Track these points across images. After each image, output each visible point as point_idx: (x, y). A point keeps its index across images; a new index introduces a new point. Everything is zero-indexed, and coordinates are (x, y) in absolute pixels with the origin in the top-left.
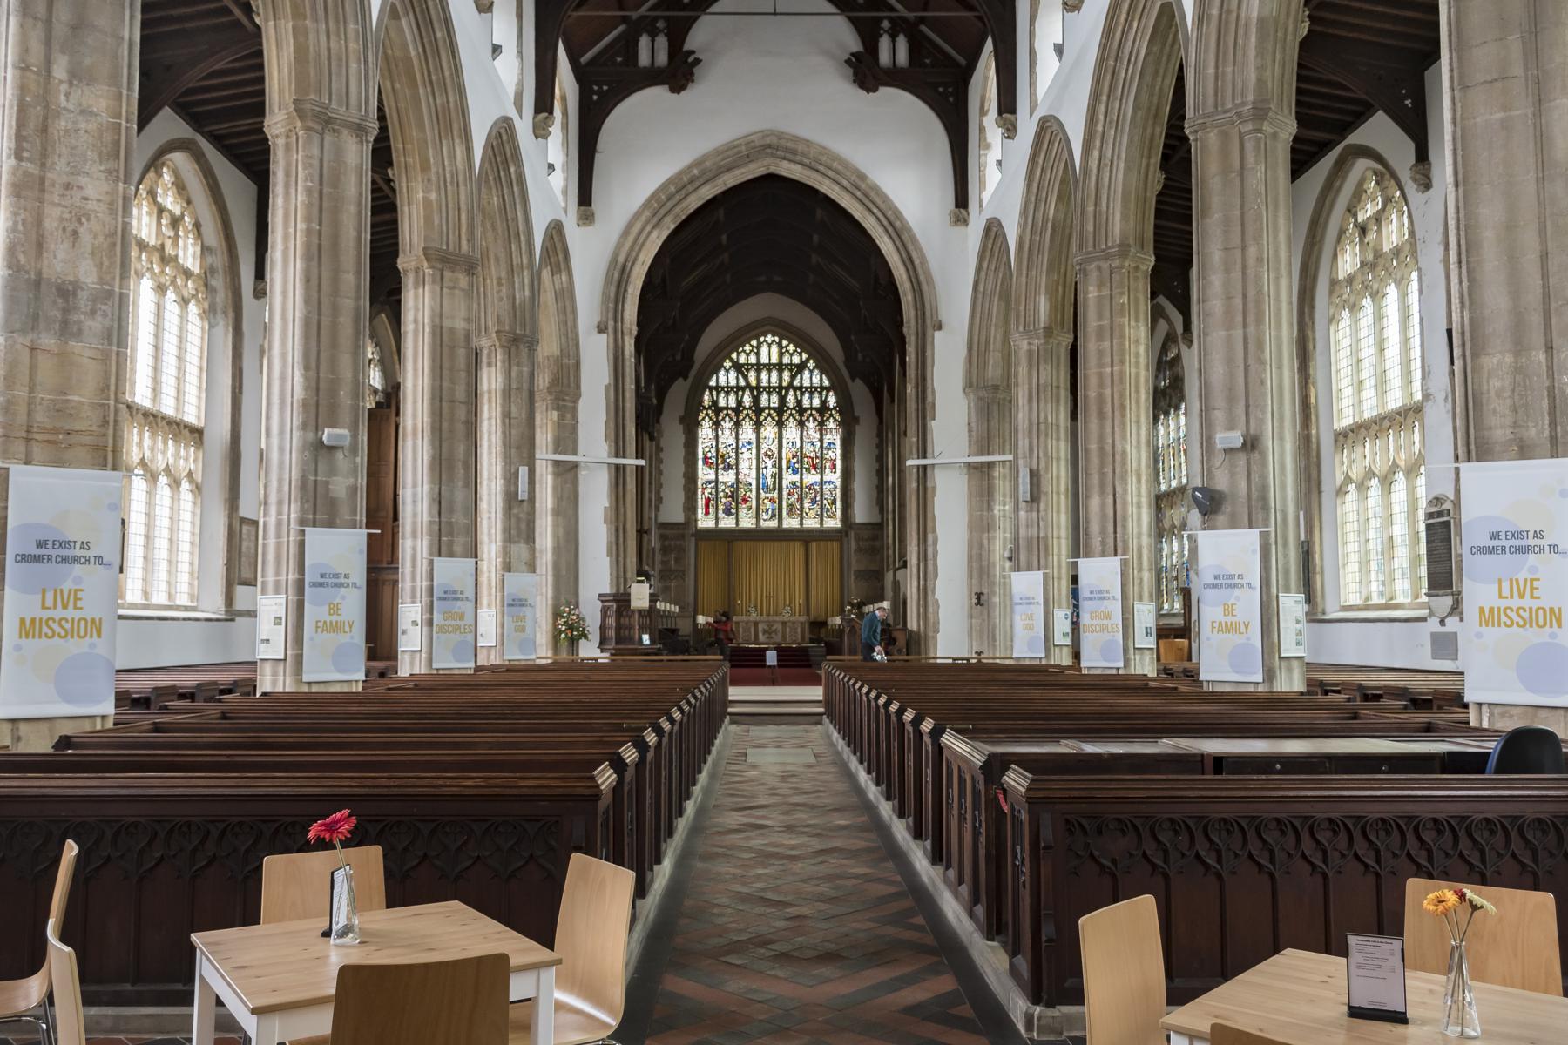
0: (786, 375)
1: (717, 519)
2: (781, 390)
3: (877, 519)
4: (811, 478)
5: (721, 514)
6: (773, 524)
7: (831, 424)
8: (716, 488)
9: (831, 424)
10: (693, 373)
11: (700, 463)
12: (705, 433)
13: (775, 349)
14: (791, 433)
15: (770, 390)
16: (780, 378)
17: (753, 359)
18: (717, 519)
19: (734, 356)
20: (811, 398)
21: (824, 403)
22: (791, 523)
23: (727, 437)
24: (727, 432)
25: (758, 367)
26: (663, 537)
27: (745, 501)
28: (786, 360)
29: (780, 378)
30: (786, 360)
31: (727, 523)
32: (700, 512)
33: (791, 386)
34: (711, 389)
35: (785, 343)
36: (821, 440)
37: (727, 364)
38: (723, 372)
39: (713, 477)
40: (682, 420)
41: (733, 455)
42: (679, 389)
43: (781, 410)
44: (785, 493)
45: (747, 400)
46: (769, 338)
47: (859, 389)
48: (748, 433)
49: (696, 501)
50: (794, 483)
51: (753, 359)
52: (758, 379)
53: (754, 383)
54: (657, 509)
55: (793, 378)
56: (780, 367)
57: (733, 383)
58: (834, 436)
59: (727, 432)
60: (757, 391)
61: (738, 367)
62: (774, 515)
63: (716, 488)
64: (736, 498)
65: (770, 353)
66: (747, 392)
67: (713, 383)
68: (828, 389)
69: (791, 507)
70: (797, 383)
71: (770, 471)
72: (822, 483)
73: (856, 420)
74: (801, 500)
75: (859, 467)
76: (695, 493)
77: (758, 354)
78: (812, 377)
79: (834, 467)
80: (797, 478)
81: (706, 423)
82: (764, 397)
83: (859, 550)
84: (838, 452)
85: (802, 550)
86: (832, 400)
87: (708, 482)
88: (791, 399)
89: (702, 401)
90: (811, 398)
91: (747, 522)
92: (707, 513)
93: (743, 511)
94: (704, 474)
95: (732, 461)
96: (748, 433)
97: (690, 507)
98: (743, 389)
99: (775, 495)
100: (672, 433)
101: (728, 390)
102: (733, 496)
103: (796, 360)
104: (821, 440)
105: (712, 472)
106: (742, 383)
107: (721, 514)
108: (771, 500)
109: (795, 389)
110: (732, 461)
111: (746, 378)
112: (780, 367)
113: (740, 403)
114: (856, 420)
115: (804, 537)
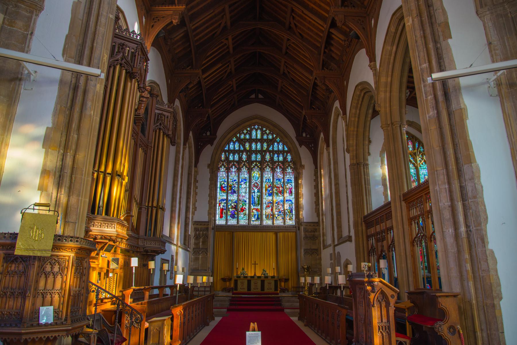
0: (265, 145)
1: (227, 220)
2: (262, 152)
3: (317, 221)
5: (229, 218)
6: (258, 223)
7: (289, 170)
8: (227, 203)
9: (289, 170)
10: (215, 142)
11: (218, 189)
12: (222, 174)
13: (259, 132)
14: (268, 175)
15: (256, 152)
16: (262, 146)
17: (248, 137)
18: (227, 220)
19: (238, 135)
20: (278, 157)
21: (285, 159)
22: (267, 222)
23: (233, 176)
24: (234, 174)
25: (251, 141)
26: (196, 230)
27: (242, 210)
28: (265, 137)
29: (262, 146)
30: (265, 137)
31: (232, 222)
32: (218, 217)
33: (268, 150)
34: (225, 151)
35: (264, 129)
37: (235, 139)
38: (232, 143)
39: (225, 197)
40: (209, 166)
41: (237, 186)
42: (208, 151)
43: (263, 162)
44: (265, 206)
45: (244, 157)
46: (256, 127)
47: (304, 153)
48: (245, 175)
49: (215, 210)
51: (248, 137)
52: (250, 147)
53: (248, 149)
54: (193, 213)
55: (268, 146)
56: (262, 141)
57: (237, 148)
58: (290, 176)
59: (234, 174)
60: (250, 152)
61: (240, 141)
62: (258, 218)
63: (227, 203)
64: (236, 210)
65: (257, 134)
66: (245, 154)
67: (226, 149)
68: (287, 152)
70: (271, 149)
71: (256, 194)
73: (303, 167)
75: (304, 191)
76: (215, 206)
77: (250, 135)
78: (279, 146)
79: (291, 192)
80: (270, 198)
81: (222, 169)
82: (253, 156)
83: (306, 237)
84: (293, 184)
85: (274, 236)
86: (289, 158)
87: (223, 200)
88: (268, 157)
89: (221, 158)
90: (278, 157)
91: (243, 222)
92: (221, 217)
93: (241, 215)
94: (221, 196)
96: (245, 175)
97: (212, 213)
98: (242, 152)
99: (259, 207)
100: (204, 173)
101: (234, 152)
102: (236, 207)
103: (270, 137)
104: (283, 178)
105: (225, 195)
106: (242, 149)
107: (229, 218)
109: (270, 152)
110: (236, 190)
111: (244, 146)
112: (262, 141)
113: (240, 158)
114: (303, 167)
115: (275, 230)
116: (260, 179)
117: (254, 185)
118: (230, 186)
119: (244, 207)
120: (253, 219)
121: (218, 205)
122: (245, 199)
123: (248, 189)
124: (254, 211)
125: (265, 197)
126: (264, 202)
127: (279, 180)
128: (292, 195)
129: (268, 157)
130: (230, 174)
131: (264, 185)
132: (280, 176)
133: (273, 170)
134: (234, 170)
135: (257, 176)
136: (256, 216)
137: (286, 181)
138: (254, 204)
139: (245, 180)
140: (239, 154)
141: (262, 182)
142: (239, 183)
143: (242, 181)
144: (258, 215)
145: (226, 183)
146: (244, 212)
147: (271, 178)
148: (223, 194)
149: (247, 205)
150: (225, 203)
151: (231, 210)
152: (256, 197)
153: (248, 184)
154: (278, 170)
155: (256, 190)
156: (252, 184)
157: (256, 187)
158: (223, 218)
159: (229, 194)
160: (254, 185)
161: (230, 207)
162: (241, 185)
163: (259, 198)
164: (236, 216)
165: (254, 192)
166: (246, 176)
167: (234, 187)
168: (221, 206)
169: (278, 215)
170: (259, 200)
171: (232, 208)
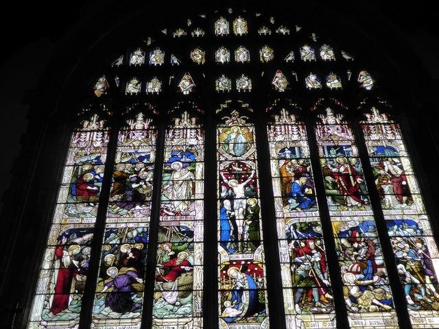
4: (351, 216)
8: (96, 245)
11: (63, 194)
14: (286, 134)
36: (360, 142)
41: (149, 176)
44: (285, 249)
48: (186, 135)
50: (308, 228)
59: (139, 136)
63: (96, 245)
69: (304, 288)
71: (239, 199)
72: (382, 225)
74: (332, 262)
80: (313, 216)
84: (406, 163)
87: (80, 232)
89: (93, 90)
92: (59, 306)
95: (146, 189)
96: (186, 135)
98: (179, 72)
99: (259, 255)
104: (360, 142)
107: (100, 308)
108: (246, 268)
109: (287, 69)
110: (146, 189)
116: (253, 149)
117: (230, 172)
118: (123, 179)
119: (182, 256)
120: (231, 312)
121: (49, 253)
122: (189, 225)
123: (200, 188)
124: (232, 271)
125: (280, 210)
126: (281, 233)
127: (340, 149)
128: (410, 201)
129: (280, 82)
130: (121, 138)
131: (274, 170)
132: (346, 137)
133: (309, 121)
134: (139, 125)
135: (242, 139)
136: (246, 298)
137: (371, 151)
138: (235, 241)
139: (189, 153)
140: (163, 80)
141: (263, 158)
142: (159, 167)
143: (174, 158)
144: (255, 293)
145: (100, 170)
146: (183, 279)
147: (305, 144)
148: (82, 208)
149: (199, 250)
150: (83, 245)
151: (112, 272)
152: (239, 214)
153: (200, 168)
154: (331, 120)
155: (239, 190)
156: (221, 167)
157: (240, 178)
158: (64, 315)
159: (112, 210)
160: (230, 172)
161: (109, 258)
162: (171, 172)
163: (255, 218)
164: (138, 299)
165: (232, 198)
166: (193, 142)
167: (139, 180)
168: (67, 259)
169: (362, 288)
170: (254, 227)
171: (122, 261)
